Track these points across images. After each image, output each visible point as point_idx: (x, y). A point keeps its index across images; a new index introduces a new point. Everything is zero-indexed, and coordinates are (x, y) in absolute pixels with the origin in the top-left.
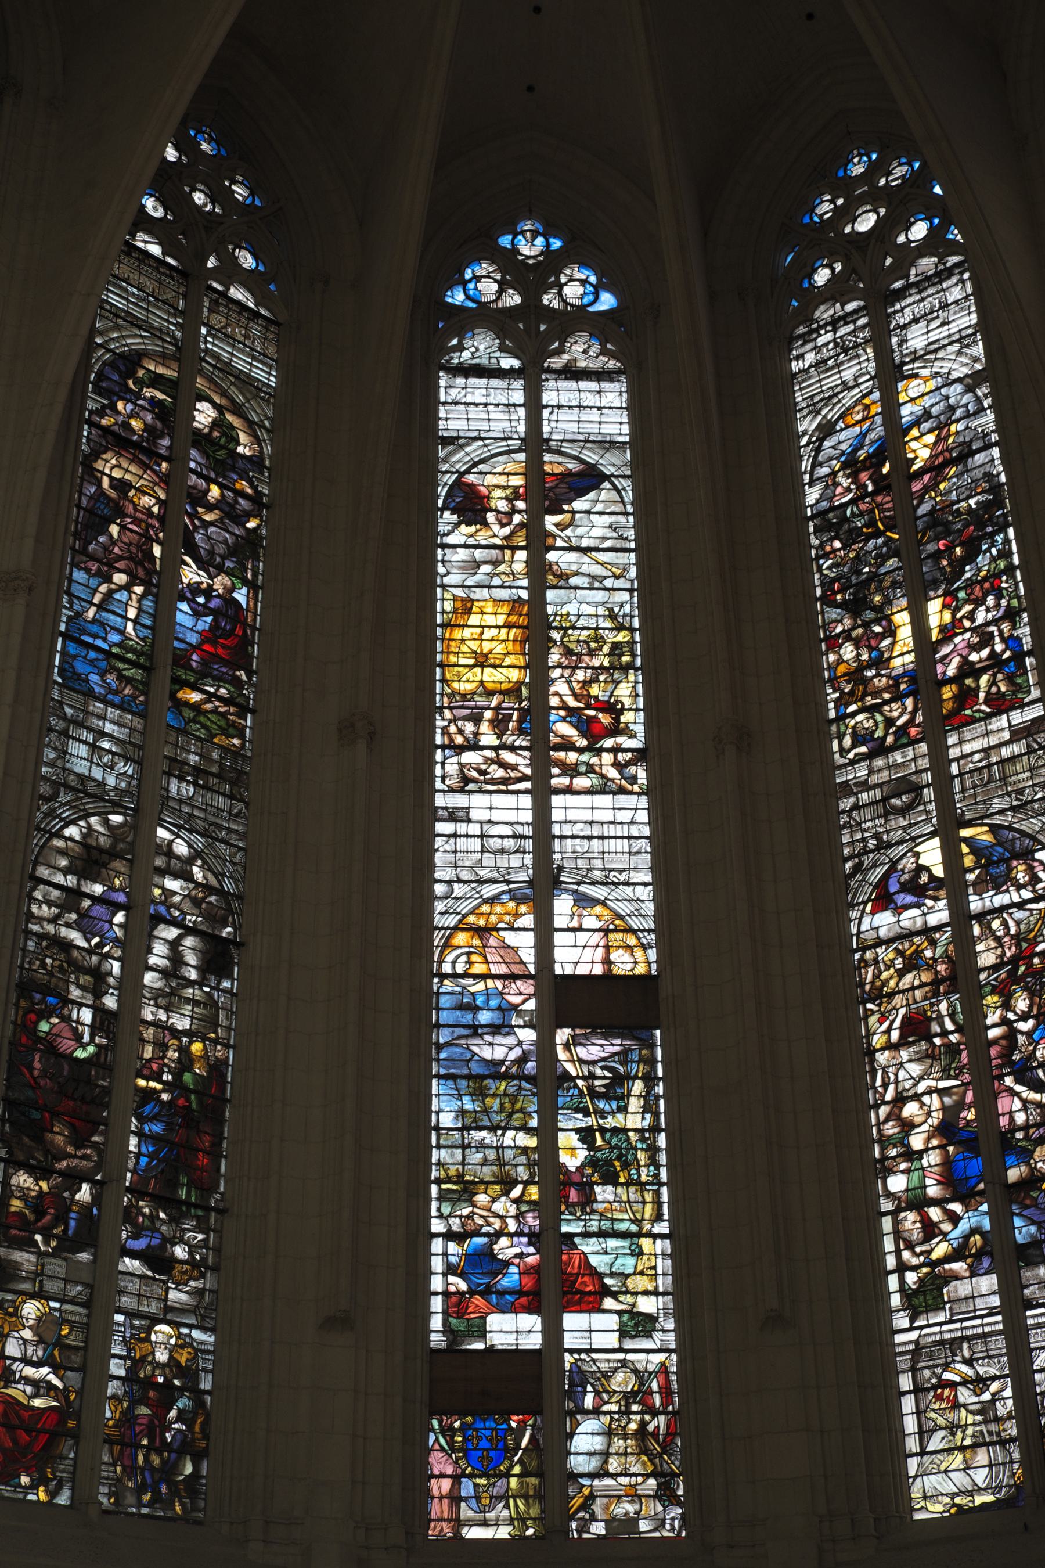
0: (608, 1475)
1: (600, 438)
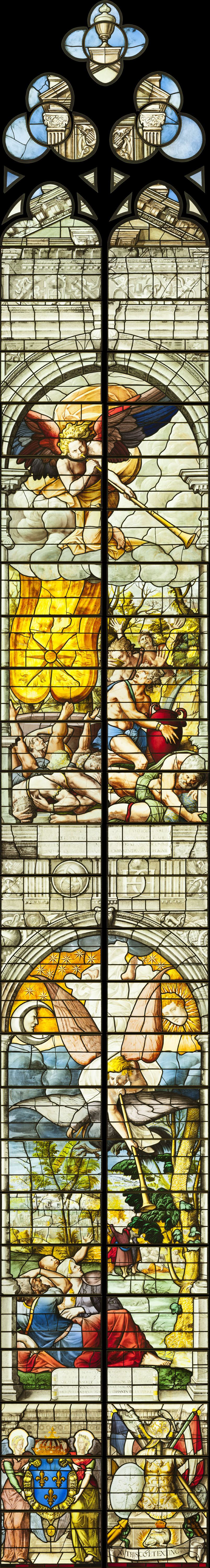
0: (142, 1510)
1: (173, 347)
